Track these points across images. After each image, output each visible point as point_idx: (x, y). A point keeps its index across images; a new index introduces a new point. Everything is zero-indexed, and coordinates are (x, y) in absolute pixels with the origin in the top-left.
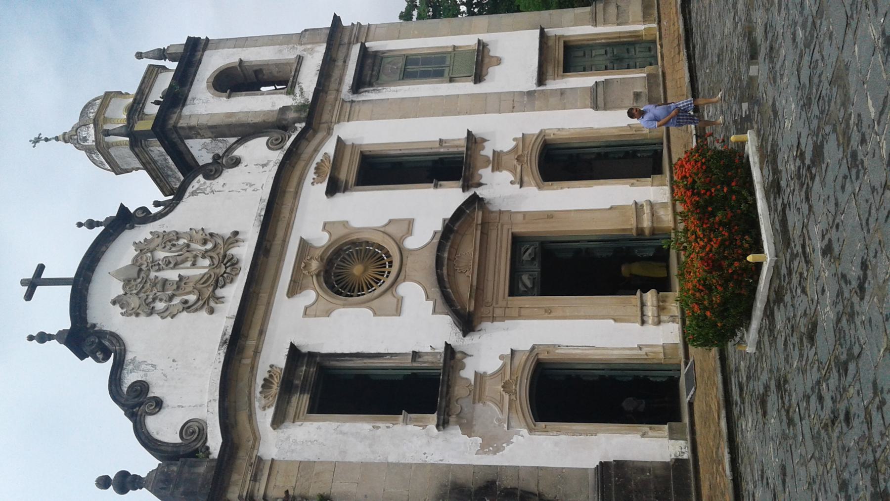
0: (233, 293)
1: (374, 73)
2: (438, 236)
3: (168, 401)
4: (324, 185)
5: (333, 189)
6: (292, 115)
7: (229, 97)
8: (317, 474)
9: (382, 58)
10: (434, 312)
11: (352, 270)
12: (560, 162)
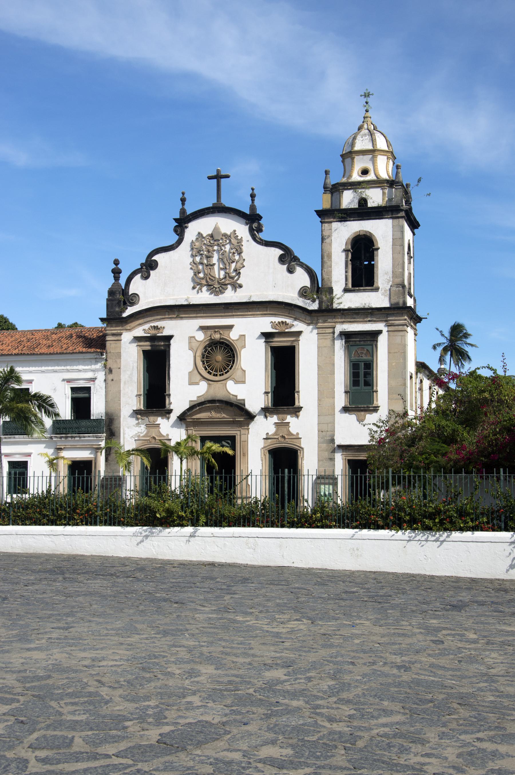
0: (205, 297)
1: (358, 342)
2: (233, 400)
4: (270, 330)
5: (267, 336)
7: (346, 251)
8: (116, 361)
9: (372, 345)
10: (191, 401)
12: (284, 459)
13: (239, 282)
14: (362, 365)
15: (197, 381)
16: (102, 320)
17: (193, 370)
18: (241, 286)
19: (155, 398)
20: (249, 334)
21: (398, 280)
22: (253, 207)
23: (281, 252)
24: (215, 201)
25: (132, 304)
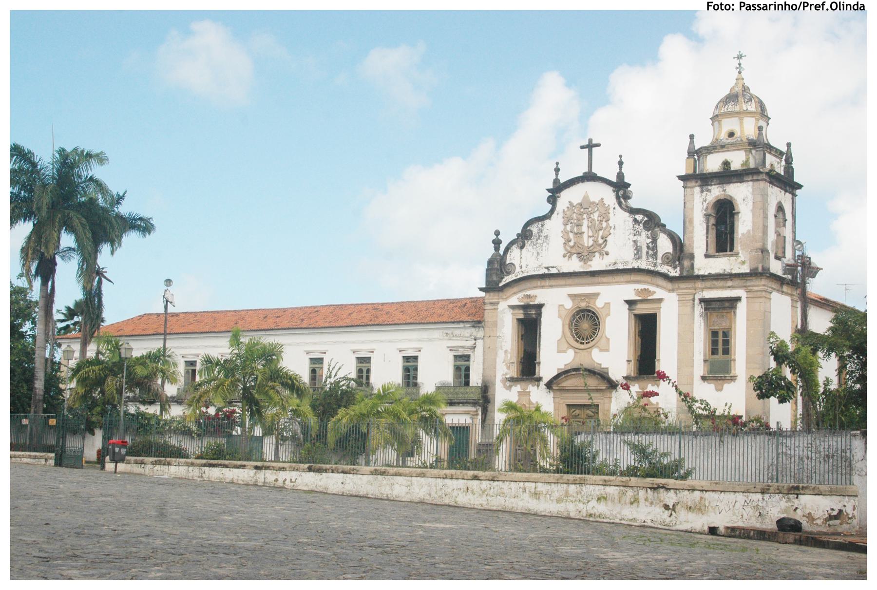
0: (575, 265)
3: (524, 250)
5: (631, 303)
6: (686, 263)
11: (585, 323)
13: (605, 249)
14: (721, 334)
16: (481, 289)
18: (607, 254)
19: (528, 366)
20: (614, 301)
21: (759, 245)
22: (620, 176)
23: (646, 219)
24: (586, 170)
25: (509, 273)
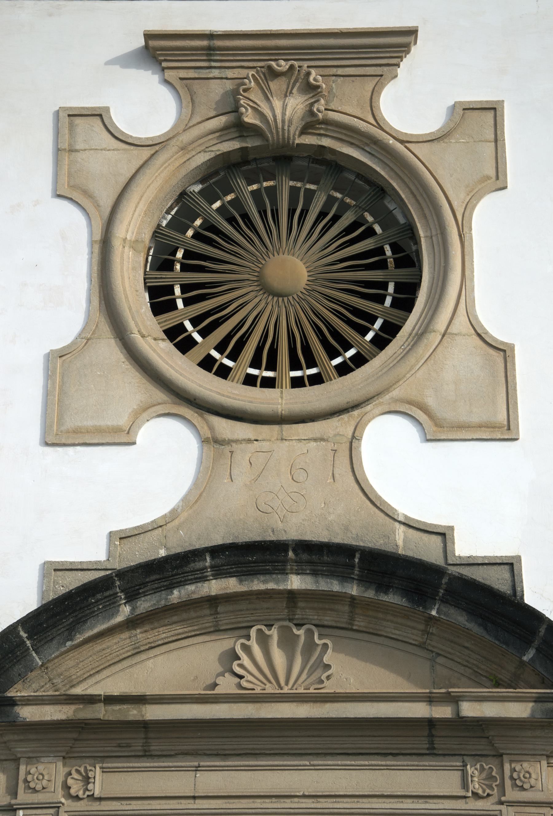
15: (123, 421)
17: (86, 339)
